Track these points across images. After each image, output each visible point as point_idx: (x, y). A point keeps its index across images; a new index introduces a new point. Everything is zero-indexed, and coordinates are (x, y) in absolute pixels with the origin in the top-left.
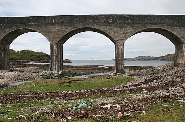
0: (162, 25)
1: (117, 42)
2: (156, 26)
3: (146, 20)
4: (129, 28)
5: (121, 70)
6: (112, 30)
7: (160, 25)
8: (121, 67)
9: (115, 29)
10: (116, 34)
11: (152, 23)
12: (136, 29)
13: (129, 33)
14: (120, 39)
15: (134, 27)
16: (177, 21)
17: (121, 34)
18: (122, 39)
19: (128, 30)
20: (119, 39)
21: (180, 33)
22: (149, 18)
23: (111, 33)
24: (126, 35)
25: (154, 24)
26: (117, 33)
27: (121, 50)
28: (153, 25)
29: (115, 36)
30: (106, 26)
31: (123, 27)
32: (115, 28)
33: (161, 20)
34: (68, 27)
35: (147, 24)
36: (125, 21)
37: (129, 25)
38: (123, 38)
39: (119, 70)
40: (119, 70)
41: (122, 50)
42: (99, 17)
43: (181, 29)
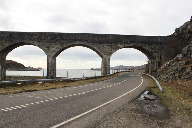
2: (80, 42)
7: (84, 42)
10: (47, 48)
12: (64, 44)
20: (49, 53)
22: (75, 36)
24: (55, 49)
27: (50, 62)
28: (78, 42)
30: (39, 41)
32: (47, 44)
34: (8, 42)
37: (58, 41)
42: (33, 34)
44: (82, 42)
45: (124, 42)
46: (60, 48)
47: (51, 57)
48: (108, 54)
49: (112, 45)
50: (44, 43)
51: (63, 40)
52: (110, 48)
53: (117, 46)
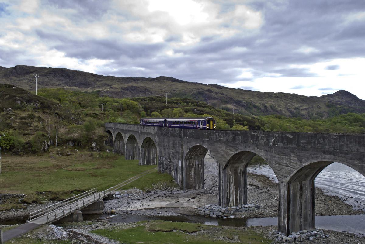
0: (344, 157)
3: (317, 145)
9: (276, 157)
10: (277, 165)
11: (327, 151)
31: (286, 156)
33: (342, 145)
37: (293, 152)
46: (297, 167)
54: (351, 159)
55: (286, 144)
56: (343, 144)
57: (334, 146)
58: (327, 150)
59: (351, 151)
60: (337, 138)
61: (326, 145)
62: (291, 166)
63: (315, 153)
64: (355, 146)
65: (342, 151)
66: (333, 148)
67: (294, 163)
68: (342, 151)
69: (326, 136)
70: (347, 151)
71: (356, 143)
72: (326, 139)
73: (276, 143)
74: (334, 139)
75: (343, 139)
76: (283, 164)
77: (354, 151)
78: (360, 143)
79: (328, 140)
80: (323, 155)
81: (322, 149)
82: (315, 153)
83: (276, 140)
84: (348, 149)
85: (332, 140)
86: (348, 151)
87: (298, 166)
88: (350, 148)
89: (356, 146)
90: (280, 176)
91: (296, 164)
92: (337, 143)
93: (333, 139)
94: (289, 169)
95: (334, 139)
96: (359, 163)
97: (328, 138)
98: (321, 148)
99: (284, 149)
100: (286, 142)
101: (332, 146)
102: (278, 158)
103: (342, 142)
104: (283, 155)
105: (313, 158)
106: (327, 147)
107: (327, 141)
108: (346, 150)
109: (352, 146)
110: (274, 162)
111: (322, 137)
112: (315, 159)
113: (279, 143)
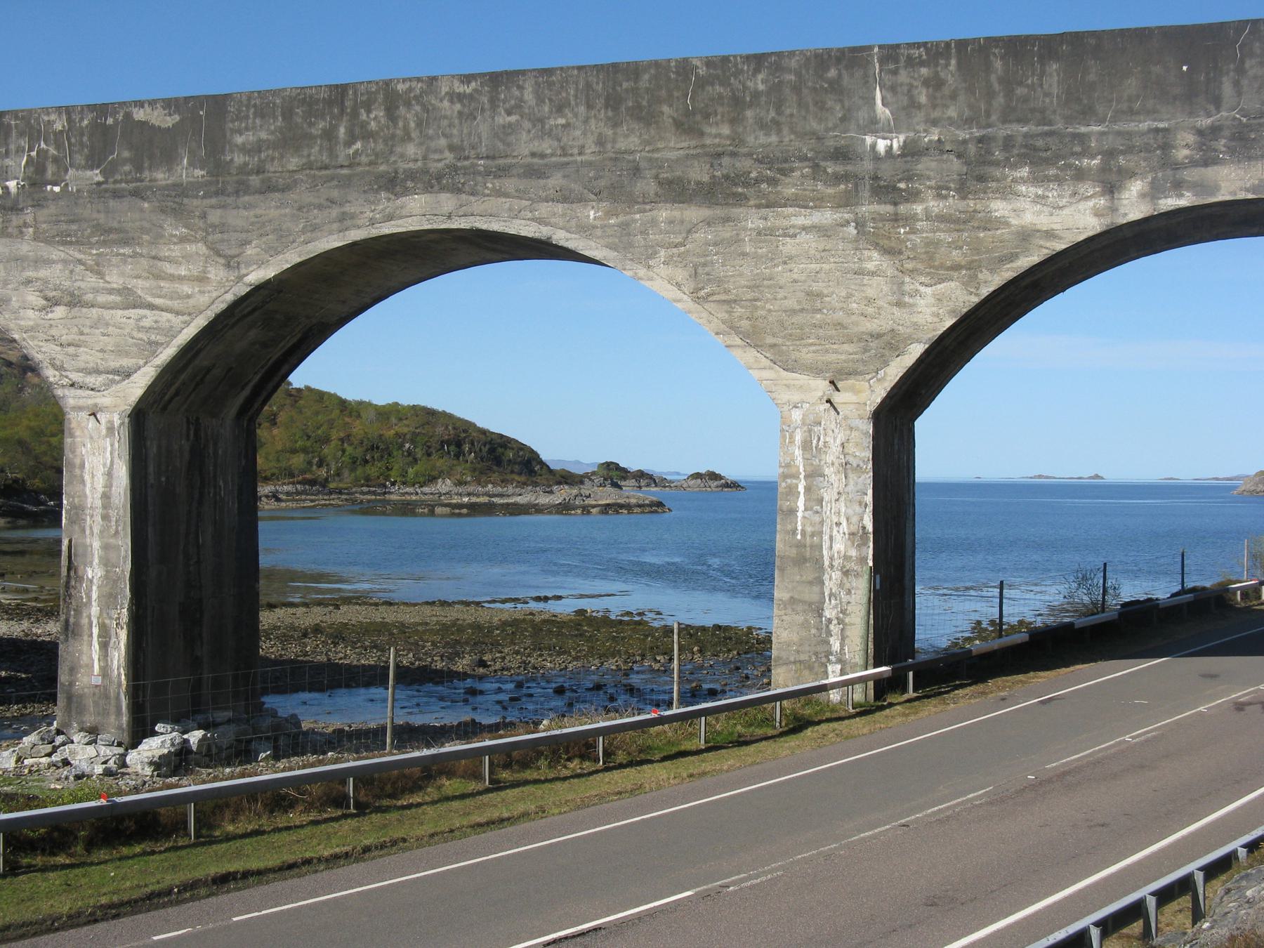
0: (521, 195)
1: (71, 398)
2: (447, 201)
3: (349, 144)
4: (176, 251)
5: (107, 697)
6: (30, 274)
7: (499, 193)
8: (105, 672)
9: (49, 262)
10: (60, 311)
11: (411, 175)
12: (250, 251)
13: (176, 304)
14: (97, 371)
15: (222, 228)
16: (687, 126)
17: (107, 314)
18: (114, 364)
19: (169, 268)
20: (89, 372)
21: (720, 282)
23: (15, 303)
24: (149, 317)
25: (432, 182)
26: (71, 305)
29: (53, 339)
31: (126, 242)
32: (56, 253)
33: (509, 129)
35: (346, 183)
36: (139, 168)
37: (178, 212)
38: (127, 354)
39: (81, 696)
40: (90, 703)
41: (109, 485)
43: (727, 232)
44: (477, 205)
45: (1110, 154)
47: (110, 429)
48: (843, 353)
49: (910, 219)
50: (25, 247)
51: (242, 188)
52: (874, 260)
53: (990, 224)
54: (565, 197)
55: (127, 168)
56: (513, 118)
57: (456, 140)
58: (411, 165)
59: (565, 155)
60: (475, 90)
61: (407, 138)
62: (158, 301)
63: (335, 194)
64: (586, 121)
65: (509, 161)
66: (451, 148)
67: (181, 279)
68: (509, 161)
69: (410, 90)
70: (536, 160)
71: (589, 106)
72: (408, 104)
73: (50, 169)
74: (454, 97)
75: (516, 93)
76: (102, 299)
77: (580, 154)
78: (613, 102)
79: (418, 108)
80: (385, 202)
81: (383, 168)
82: (335, 194)
83: (52, 151)
84: (546, 146)
85: (446, 104)
86: (543, 156)
87: (549, 180)
88: (559, 140)
89: (593, 121)
90: (75, 377)
91: (202, 279)
92: (475, 118)
93: (452, 101)
94: (146, 323)
95: (454, 97)
96: (609, 214)
97: (416, 97)
98: (371, 163)
99: (112, 203)
100: (126, 154)
101: (443, 142)
102: (65, 262)
103: (509, 113)
104: (104, 243)
105: (315, 228)
106: (411, 150)
107: (409, 116)
108: (533, 155)
109: (566, 126)
110: (34, 298)
111: (381, 97)
112: (331, 233)
113: (71, 172)
